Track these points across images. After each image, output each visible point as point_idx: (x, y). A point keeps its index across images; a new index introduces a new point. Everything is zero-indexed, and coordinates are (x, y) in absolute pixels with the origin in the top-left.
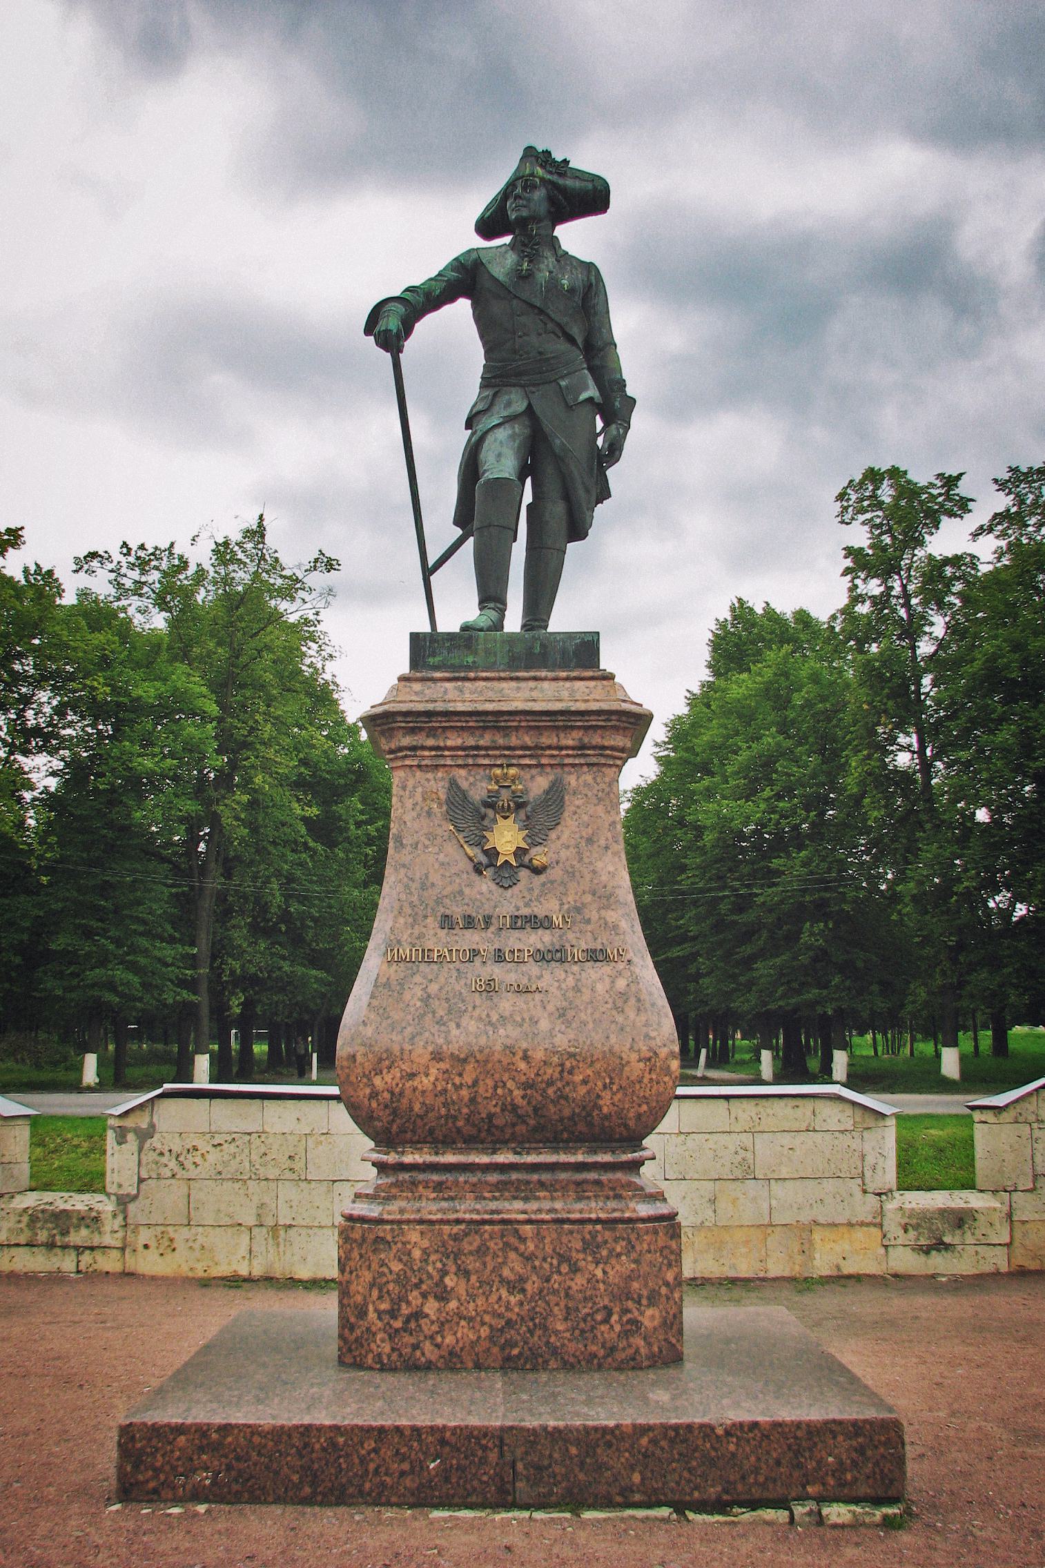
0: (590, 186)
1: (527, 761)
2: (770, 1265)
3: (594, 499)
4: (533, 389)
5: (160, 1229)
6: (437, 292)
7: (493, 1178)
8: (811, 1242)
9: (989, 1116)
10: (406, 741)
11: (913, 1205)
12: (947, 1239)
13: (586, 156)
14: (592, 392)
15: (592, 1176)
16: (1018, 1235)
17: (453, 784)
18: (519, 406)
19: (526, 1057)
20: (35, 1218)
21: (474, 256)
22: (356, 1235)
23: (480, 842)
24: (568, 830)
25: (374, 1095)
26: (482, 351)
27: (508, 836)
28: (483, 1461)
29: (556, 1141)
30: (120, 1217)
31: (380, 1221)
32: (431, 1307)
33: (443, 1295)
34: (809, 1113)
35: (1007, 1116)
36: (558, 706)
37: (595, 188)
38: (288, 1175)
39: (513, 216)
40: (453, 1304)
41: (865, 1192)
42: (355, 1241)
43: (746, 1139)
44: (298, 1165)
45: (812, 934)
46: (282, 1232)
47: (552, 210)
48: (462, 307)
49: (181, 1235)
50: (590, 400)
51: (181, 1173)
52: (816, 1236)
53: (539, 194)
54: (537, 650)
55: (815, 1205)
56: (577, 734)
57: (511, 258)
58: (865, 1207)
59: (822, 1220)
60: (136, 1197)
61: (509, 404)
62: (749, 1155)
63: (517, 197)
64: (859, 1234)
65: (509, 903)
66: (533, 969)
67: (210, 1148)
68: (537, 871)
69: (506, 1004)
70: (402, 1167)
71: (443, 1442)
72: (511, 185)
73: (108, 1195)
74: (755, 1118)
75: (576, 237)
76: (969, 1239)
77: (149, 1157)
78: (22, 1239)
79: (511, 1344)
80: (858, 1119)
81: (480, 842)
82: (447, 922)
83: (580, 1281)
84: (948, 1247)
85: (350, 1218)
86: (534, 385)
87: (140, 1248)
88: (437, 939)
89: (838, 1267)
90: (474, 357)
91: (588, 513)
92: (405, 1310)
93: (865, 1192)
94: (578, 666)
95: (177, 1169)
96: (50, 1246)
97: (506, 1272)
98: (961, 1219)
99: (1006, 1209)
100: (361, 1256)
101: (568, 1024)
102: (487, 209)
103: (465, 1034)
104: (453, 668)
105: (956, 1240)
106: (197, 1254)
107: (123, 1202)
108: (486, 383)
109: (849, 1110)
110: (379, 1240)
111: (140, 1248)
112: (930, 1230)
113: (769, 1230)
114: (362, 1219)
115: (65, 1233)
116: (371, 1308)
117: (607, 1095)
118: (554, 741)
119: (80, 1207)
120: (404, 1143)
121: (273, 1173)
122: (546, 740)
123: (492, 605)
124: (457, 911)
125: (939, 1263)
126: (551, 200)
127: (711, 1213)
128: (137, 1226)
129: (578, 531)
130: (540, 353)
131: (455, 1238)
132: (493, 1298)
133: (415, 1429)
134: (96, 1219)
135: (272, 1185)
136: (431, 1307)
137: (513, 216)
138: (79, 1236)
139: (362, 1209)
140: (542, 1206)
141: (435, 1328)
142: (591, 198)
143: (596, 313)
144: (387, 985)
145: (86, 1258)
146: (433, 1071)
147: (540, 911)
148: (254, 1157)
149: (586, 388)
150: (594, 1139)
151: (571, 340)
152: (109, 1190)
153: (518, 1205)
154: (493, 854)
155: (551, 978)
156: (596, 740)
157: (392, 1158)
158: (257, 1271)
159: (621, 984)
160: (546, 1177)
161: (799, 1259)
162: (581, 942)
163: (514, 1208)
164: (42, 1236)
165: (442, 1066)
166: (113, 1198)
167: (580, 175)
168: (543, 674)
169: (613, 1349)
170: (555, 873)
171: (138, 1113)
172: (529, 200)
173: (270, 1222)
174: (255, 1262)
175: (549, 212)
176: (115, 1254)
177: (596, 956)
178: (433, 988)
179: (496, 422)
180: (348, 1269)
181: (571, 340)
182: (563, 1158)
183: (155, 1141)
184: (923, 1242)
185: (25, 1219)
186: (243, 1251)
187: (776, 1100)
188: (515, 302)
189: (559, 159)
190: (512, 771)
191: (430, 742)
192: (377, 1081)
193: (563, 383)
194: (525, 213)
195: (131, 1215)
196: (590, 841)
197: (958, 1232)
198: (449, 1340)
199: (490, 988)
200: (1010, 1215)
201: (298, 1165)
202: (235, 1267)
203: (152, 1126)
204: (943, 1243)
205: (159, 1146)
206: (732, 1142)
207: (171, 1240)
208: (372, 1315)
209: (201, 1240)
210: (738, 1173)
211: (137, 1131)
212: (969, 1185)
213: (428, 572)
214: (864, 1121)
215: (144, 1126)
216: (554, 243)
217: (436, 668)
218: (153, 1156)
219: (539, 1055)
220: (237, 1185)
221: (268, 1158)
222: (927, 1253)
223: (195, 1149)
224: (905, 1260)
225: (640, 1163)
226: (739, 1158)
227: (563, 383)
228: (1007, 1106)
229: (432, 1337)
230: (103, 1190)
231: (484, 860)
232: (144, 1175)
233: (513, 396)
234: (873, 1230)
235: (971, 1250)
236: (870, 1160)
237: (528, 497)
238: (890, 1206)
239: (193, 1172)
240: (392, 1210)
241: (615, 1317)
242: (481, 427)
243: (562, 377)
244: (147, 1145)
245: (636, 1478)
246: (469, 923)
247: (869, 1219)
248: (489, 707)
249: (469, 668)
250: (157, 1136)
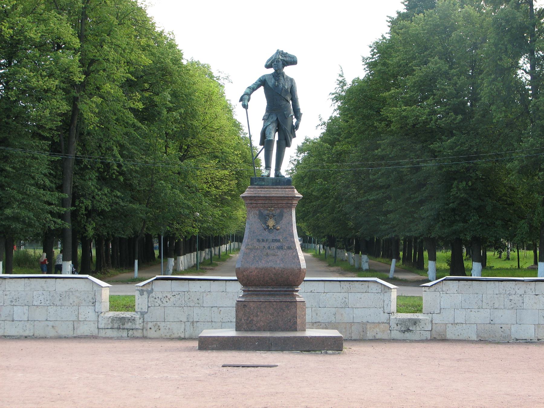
5: (155, 323)
7: (268, 293)
8: (366, 329)
9: (426, 289)
10: (250, 202)
11: (400, 317)
12: (410, 328)
15: (288, 293)
16: (434, 327)
17: (260, 211)
18: (275, 119)
19: (274, 268)
20: (113, 320)
22: (239, 305)
23: (265, 223)
24: (284, 221)
25: (244, 276)
27: (271, 222)
28: (266, 343)
29: (280, 285)
30: (142, 319)
31: (245, 301)
32: (255, 319)
33: (257, 316)
34: (367, 286)
35: (432, 289)
36: (282, 195)
38: (197, 305)
40: (259, 318)
41: (384, 312)
43: (346, 295)
44: (200, 302)
45: (459, 190)
46: (195, 324)
49: (162, 325)
51: (162, 305)
52: (368, 327)
57: (273, 81)
58: (384, 318)
60: (147, 312)
61: (272, 118)
62: (347, 300)
64: (382, 326)
65: (271, 237)
66: (276, 251)
67: (171, 296)
68: (277, 230)
69: (270, 258)
70: (249, 291)
71: (258, 339)
73: (137, 312)
76: (418, 329)
77: (151, 299)
78: (109, 327)
79: (270, 326)
81: (265, 223)
82: (258, 240)
83: (285, 313)
84: (411, 331)
85: (238, 301)
87: (148, 329)
88: (256, 244)
89: (375, 336)
92: (250, 319)
93: (384, 312)
94: (287, 185)
95: (160, 303)
96: (119, 328)
97: (270, 312)
98: (415, 322)
99: (430, 319)
101: (283, 262)
102: (267, 62)
103: (262, 264)
104: (260, 185)
105: (414, 329)
106: (167, 330)
107: (143, 314)
109: (380, 286)
110: (245, 305)
111: (148, 329)
112: (405, 325)
113: (353, 324)
114: (241, 301)
115: (123, 324)
117: (291, 276)
118: (281, 202)
119: (128, 316)
120: (249, 286)
121: (192, 304)
122: (279, 202)
124: (261, 238)
125: (407, 335)
127: (333, 318)
128: (148, 322)
131: (260, 305)
133: (253, 337)
134: (134, 320)
135: (192, 308)
136: (255, 319)
138: (128, 325)
139: (240, 299)
140: (277, 299)
142: (292, 61)
144: (246, 254)
145: (131, 332)
147: (277, 238)
148: (186, 299)
150: (288, 285)
152: (136, 310)
153: (273, 298)
155: (280, 253)
156: (290, 202)
157: (247, 289)
158: (187, 336)
159: (294, 254)
160: (278, 293)
162: (286, 245)
163: (272, 299)
164: (116, 326)
166: (139, 313)
168: (279, 187)
169: (291, 327)
170: (281, 230)
171: (147, 285)
173: (191, 320)
174: (186, 333)
176: (140, 331)
177: (289, 248)
178: (256, 254)
182: (282, 289)
183: (153, 294)
184: (403, 329)
185: (110, 320)
186: (182, 330)
190: (272, 209)
191: (255, 202)
192: (244, 273)
195: (145, 318)
196: (288, 223)
197: (414, 326)
198: (259, 325)
199: (267, 255)
200: (432, 321)
201: (200, 302)
202: (180, 335)
203: (152, 289)
204: (409, 330)
205: (154, 296)
206: (342, 295)
207: (159, 326)
208: (243, 320)
209: (168, 326)
210: (343, 306)
211: (147, 291)
212: (420, 311)
214: (384, 290)
215: (150, 289)
217: (256, 185)
218: (153, 299)
219: (277, 268)
220: (180, 308)
221: (190, 300)
222: (404, 333)
223: (167, 297)
224: (396, 334)
226: (343, 301)
228: (432, 285)
230: (134, 310)
231: (266, 227)
232: (150, 305)
234: (386, 324)
235: (418, 332)
236: (386, 302)
238: (392, 317)
239: (166, 304)
240: (248, 299)
244: (151, 295)
245: (294, 346)
246: (263, 241)
247: (385, 321)
248: (268, 195)
249: (263, 185)
250: (154, 293)
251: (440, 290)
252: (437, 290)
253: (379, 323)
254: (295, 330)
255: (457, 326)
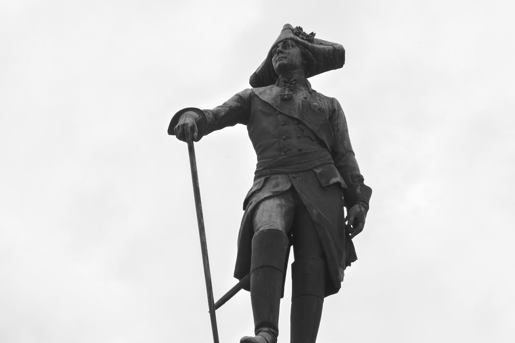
0: (331, 47)
3: (343, 262)
4: (294, 175)
6: (223, 113)
13: (325, 34)
14: (338, 179)
18: (285, 186)
21: (249, 92)
26: (256, 156)
37: (334, 48)
39: (276, 65)
47: (305, 62)
48: (240, 130)
50: (338, 184)
53: (295, 52)
61: (277, 185)
63: (280, 52)
72: (276, 46)
75: (321, 83)
86: (296, 173)
90: (249, 159)
91: (340, 269)
102: (258, 69)
108: (258, 174)
123: (266, 329)
126: (304, 55)
129: (333, 286)
130: (300, 150)
137: (276, 65)
143: (338, 130)
149: (335, 176)
151: (322, 143)
167: (321, 42)
172: (289, 53)
175: (303, 64)
179: (267, 195)
181: (322, 143)
188: (279, 117)
189: (308, 32)
193: (318, 171)
194: (285, 61)
213: (213, 307)
216: (307, 85)
227: (318, 171)
233: (279, 180)
237: (291, 259)
242: (254, 200)
243: (317, 167)
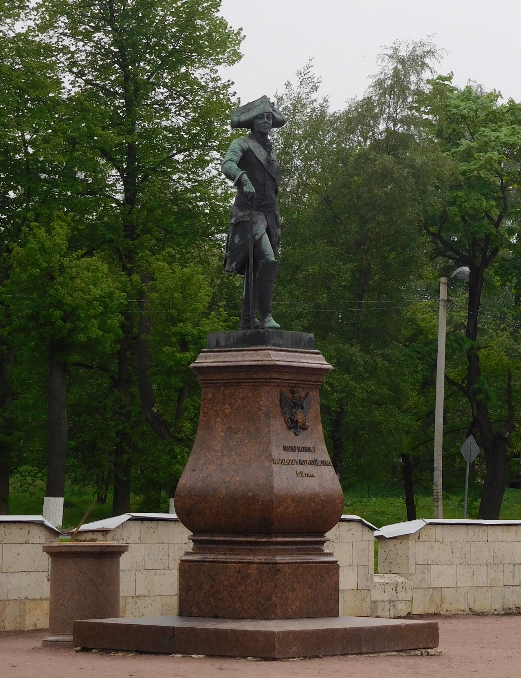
1: (301, 386)
2: (7, 625)
33: (293, 590)
40: (296, 593)
42: (265, 571)
54: (298, 340)
55: (27, 588)
56: (316, 377)
59: (30, 597)
74: (4, 535)
80: (48, 536)
82: (286, 449)
100: (268, 577)
116: (274, 596)
124: (287, 444)
132: (305, 590)
141: (291, 603)
146: (292, 506)
154: (297, 422)
161: (19, 619)
165: (294, 504)
180: (260, 583)
187: (13, 524)
219: (317, 501)
225: (324, 542)
229: (291, 607)
241: (333, 597)
251: (120, 537)
252: (115, 538)
253: (41, 599)
254: (116, 616)
255: (138, 601)
